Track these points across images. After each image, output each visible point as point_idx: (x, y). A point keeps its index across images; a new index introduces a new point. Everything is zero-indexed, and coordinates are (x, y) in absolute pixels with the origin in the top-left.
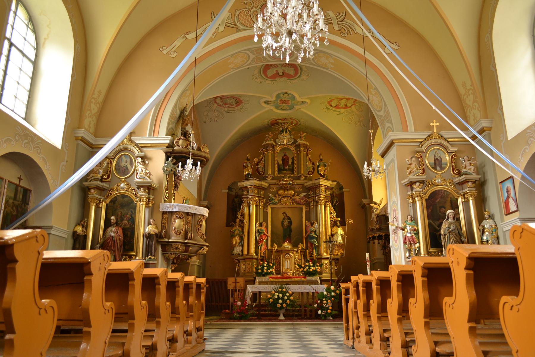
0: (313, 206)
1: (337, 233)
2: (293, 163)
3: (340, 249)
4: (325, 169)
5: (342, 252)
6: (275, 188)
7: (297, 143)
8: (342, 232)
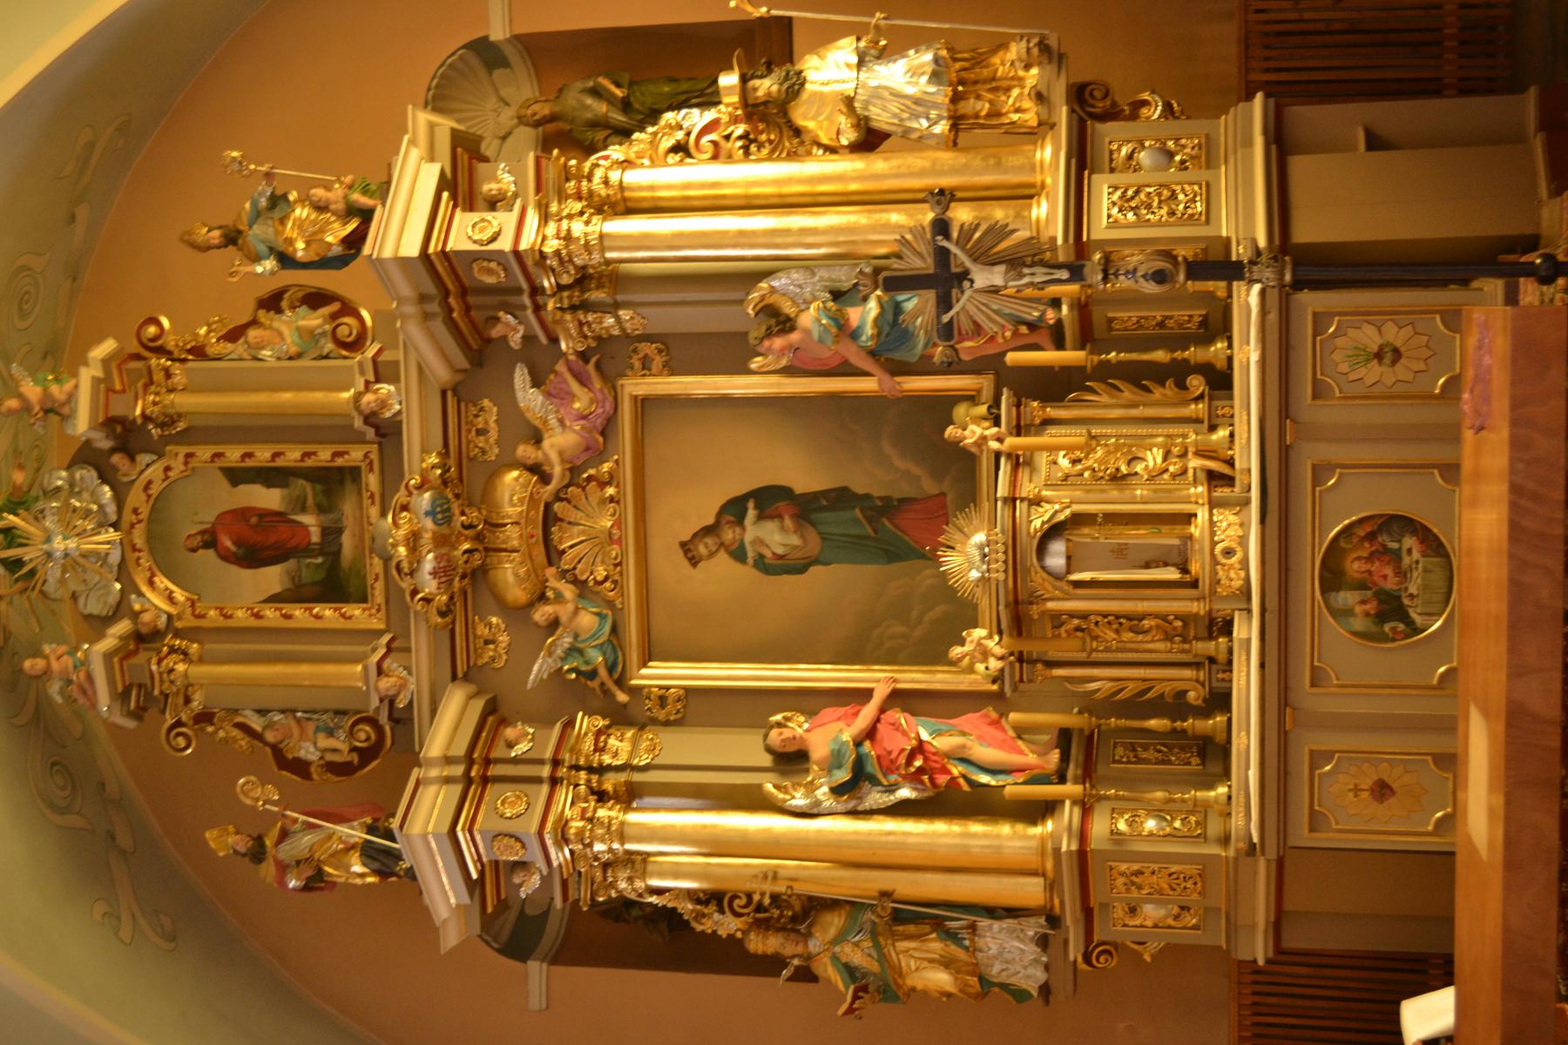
0: (625, 314)
1: (849, 101)
2: (270, 476)
3: (986, 73)
4: (301, 201)
5: (1015, 51)
6: (482, 630)
7: (103, 443)
8: (844, 51)
